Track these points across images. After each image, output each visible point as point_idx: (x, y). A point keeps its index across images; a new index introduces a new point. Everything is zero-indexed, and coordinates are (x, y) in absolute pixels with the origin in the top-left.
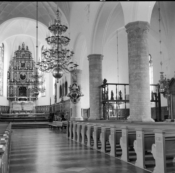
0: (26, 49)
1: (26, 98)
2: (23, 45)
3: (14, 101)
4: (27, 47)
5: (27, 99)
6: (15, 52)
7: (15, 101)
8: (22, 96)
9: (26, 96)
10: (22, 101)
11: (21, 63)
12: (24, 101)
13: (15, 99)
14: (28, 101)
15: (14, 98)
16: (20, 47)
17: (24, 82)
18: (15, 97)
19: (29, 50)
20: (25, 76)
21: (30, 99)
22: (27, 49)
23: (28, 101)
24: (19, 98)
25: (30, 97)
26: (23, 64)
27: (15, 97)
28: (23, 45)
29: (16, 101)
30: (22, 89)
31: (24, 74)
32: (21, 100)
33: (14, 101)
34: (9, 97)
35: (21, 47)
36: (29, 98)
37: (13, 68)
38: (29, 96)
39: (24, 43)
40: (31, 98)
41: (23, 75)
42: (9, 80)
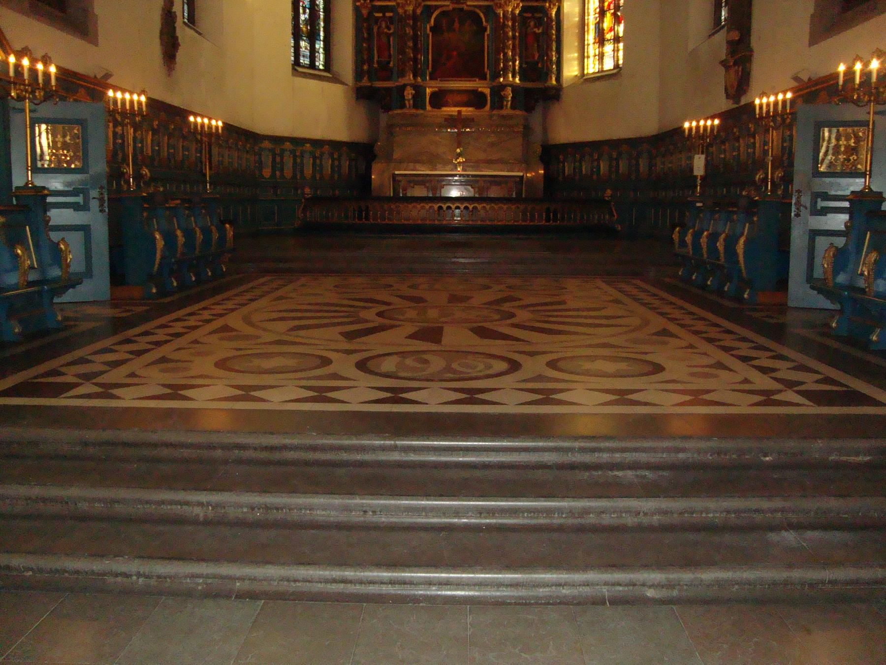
3: (403, 106)
5: (487, 91)
7: (409, 111)
9: (483, 78)
10: (453, 110)
13: (409, 93)
18: (409, 78)
23: (492, 108)
27: (409, 78)
29: (415, 106)
32: (447, 105)
33: (403, 106)
34: (365, 82)
36: (503, 87)
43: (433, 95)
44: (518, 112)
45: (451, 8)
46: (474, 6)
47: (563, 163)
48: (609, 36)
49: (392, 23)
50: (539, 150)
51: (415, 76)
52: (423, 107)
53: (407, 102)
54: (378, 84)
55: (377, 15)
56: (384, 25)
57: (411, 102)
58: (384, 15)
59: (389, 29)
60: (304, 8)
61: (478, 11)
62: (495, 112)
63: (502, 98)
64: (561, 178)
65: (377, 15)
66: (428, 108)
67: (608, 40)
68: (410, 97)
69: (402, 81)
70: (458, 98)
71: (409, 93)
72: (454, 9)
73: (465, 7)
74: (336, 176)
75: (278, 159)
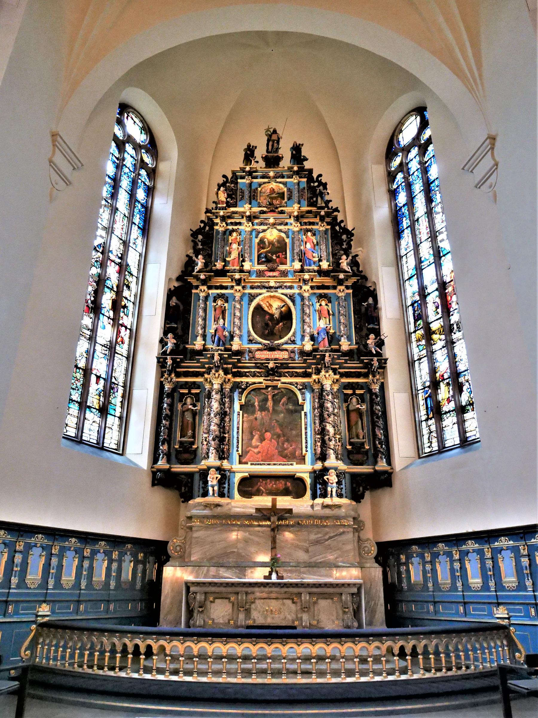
0: (286, 163)
1: (304, 470)
2: (273, 138)
3: (205, 494)
4: (297, 150)
6: (224, 184)
8: (268, 459)
9: (302, 460)
10: (265, 501)
11: (262, 241)
12: (284, 502)
13: (213, 479)
14: (314, 497)
15: (204, 474)
16: (249, 154)
17: (277, 354)
19: (307, 165)
20: (287, 316)
21: (332, 478)
22: (293, 157)
23: (314, 497)
24: (240, 470)
25: (332, 461)
26: (271, 243)
28: (273, 138)
29: (221, 495)
30: (263, 408)
31: (276, 304)
32: (258, 493)
34: (162, 464)
35: (261, 152)
37: (206, 265)
38: (323, 457)
39: (275, 132)
40: (340, 475)
41: (275, 308)
42: (171, 343)
43: (243, 480)
44: (344, 501)
45: (263, 385)
46: (291, 384)
47: (406, 564)
48: (447, 407)
49: (198, 400)
50: (374, 550)
51: (221, 458)
52: (230, 496)
53: (210, 489)
54: (178, 468)
55: (182, 391)
56: (189, 401)
57: (216, 488)
58: (189, 391)
59: (195, 406)
60: (98, 377)
61: (293, 388)
62: (319, 501)
63: (325, 484)
64: (405, 585)
65: (182, 391)
66: (237, 495)
67: (446, 413)
68: (215, 482)
69: (204, 464)
70: (271, 485)
71: (213, 479)
72: (267, 387)
73: (280, 385)
74: (113, 584)
75: (18, 558)
